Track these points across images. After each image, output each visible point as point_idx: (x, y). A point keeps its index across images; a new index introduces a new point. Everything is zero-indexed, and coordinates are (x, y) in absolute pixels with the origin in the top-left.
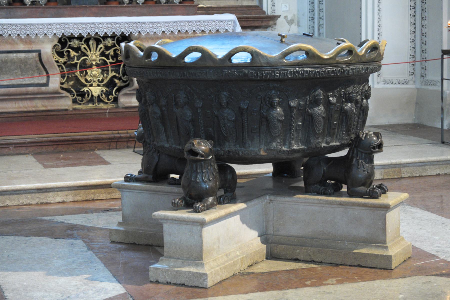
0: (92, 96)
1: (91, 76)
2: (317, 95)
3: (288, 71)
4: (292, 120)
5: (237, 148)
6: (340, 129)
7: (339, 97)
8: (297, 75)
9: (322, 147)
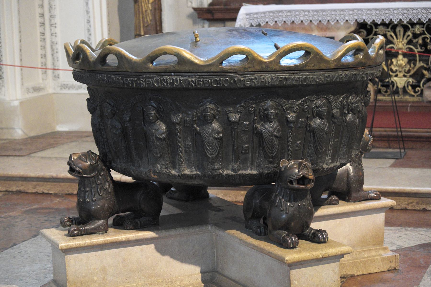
0: (397, 87)
1: (396, 65)
3: (153, 79)
4: (177, 140)
5: (128, 166)
7: (246, 115)
8: (165, 84)
9: (224, 175)
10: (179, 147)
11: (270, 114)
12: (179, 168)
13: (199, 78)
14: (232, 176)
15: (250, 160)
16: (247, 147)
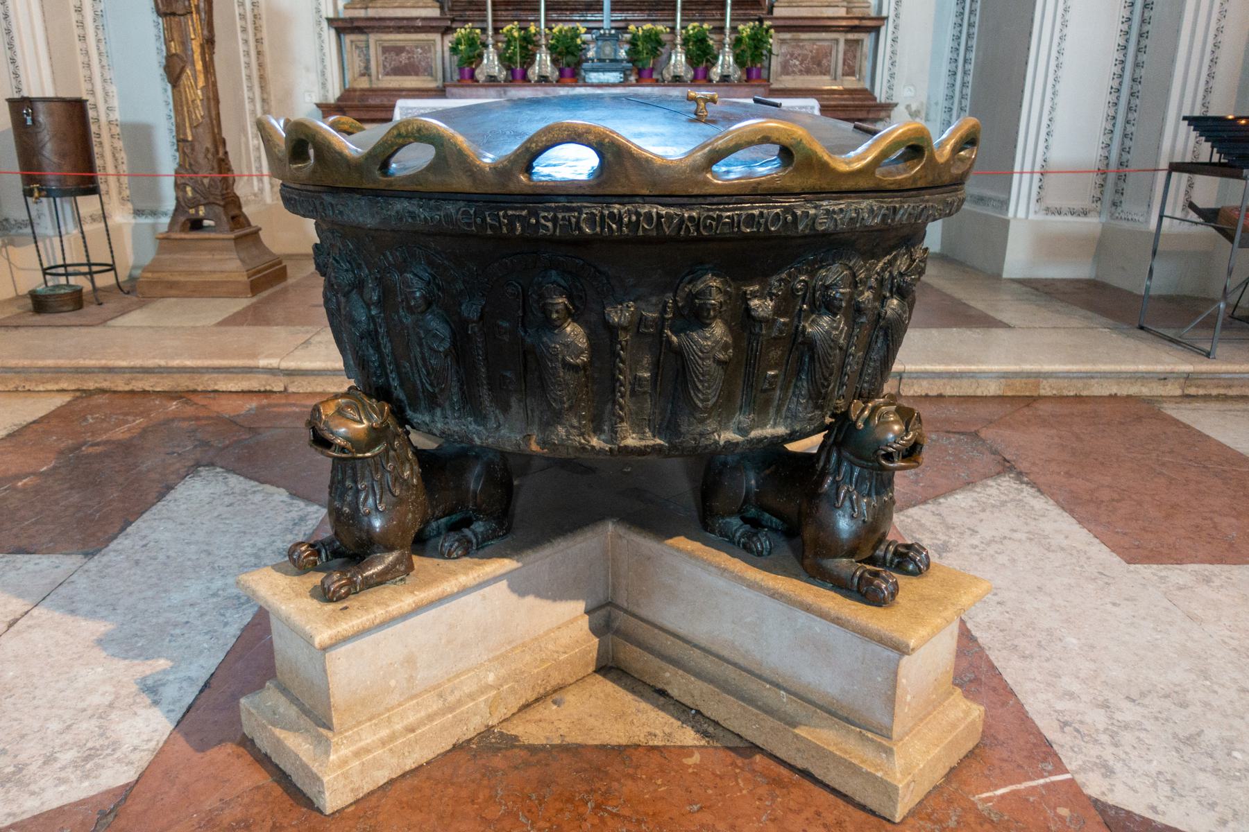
2: (701, 294)
3: (580, 214)
6: (791, 391)
7: (786, 304)
8: (614, 226)
9: (722, 443)
10: (618, 384)
11: (838, 296)
12: (614, 431)
13: (709, 210)
14: (737, 444)
15: (776, 403)
16: (774, 376)
